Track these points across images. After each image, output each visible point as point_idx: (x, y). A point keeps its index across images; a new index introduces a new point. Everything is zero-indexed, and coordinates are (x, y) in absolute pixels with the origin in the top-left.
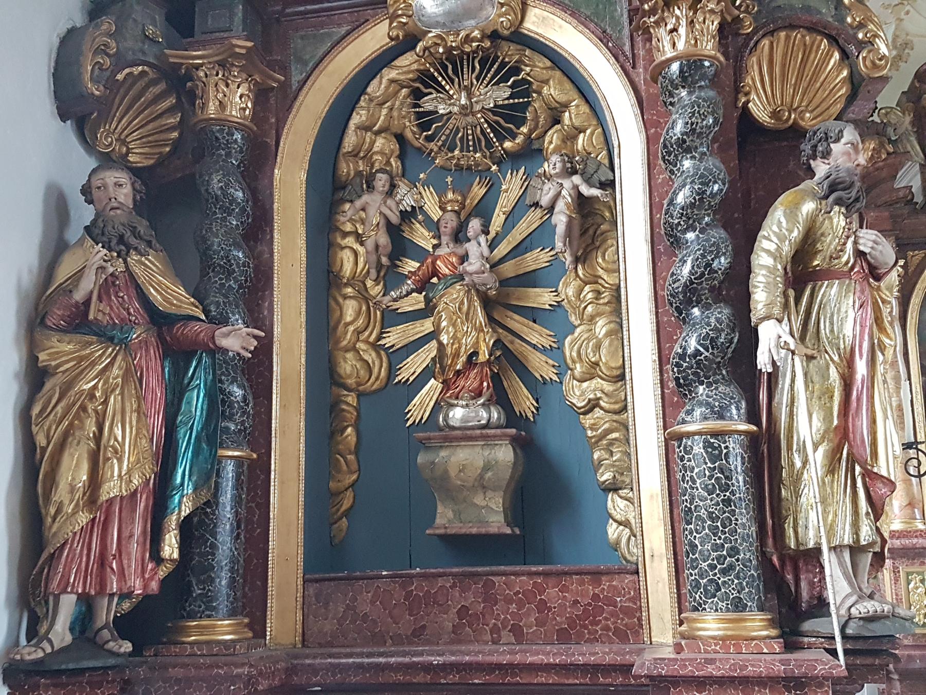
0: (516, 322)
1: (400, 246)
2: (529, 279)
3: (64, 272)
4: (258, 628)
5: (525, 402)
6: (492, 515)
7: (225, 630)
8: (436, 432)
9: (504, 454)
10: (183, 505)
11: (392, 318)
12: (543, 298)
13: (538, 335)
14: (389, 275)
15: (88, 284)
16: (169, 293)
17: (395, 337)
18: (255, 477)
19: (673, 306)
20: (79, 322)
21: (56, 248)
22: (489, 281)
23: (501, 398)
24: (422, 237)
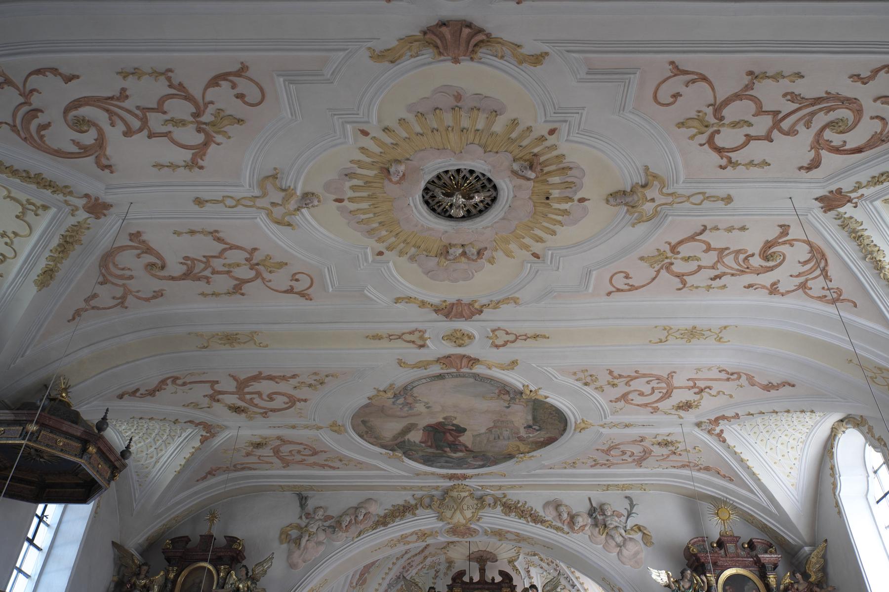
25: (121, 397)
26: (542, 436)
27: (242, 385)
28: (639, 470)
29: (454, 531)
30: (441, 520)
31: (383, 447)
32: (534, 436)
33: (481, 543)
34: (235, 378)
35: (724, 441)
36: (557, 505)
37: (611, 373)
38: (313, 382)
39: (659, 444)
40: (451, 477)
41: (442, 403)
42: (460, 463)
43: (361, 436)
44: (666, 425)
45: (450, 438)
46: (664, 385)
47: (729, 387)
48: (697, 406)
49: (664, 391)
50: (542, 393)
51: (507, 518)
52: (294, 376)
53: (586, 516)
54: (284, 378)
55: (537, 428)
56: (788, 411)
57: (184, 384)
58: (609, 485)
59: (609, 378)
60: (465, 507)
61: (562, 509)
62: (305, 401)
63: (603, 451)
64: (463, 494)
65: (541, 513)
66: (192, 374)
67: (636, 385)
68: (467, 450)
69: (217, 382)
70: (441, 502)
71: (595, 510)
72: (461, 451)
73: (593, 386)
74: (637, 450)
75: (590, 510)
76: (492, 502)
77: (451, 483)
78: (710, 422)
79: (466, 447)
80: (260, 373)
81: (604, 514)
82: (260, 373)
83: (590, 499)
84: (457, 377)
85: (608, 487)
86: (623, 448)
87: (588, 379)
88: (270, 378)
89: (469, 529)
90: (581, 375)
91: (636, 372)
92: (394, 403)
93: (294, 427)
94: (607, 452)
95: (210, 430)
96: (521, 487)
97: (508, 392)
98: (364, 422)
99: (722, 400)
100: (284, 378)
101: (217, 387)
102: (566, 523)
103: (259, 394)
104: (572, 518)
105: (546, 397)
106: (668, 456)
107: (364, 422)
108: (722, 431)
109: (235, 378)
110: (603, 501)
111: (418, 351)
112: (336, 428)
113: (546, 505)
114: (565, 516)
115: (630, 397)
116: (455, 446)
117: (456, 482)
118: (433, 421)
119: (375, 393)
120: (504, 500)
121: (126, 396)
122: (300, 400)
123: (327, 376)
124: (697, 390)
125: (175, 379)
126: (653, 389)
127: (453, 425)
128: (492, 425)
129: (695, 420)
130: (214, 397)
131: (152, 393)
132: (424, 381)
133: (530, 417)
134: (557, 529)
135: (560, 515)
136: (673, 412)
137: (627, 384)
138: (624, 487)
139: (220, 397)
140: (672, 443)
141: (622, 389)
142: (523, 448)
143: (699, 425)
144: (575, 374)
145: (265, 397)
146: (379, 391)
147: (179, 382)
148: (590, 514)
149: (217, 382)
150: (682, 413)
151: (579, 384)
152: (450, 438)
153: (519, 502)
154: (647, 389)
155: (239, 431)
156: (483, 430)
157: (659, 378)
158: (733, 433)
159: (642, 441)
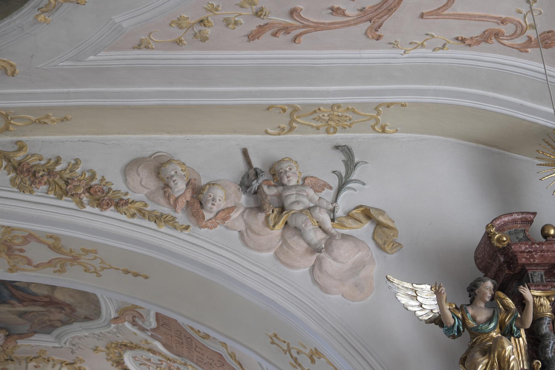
28: (376, 55)
36: (159, 167)
51: (26, 197)
53: (234, 188)
58: (295, 109)
61: (170, 170)
65: (118, 184)
71: (257, 174)
75: (247, 175)
83: (245, 152)
102: (182, 203)
104: (198, 196)
110: (279, 155)
113: (135, 164)
114: (180, 187)
120: (19, 157)
134: (158, 218)
135: (167, 186)
138: (332, 118)
148: (245, 185)
153: (58, 161)
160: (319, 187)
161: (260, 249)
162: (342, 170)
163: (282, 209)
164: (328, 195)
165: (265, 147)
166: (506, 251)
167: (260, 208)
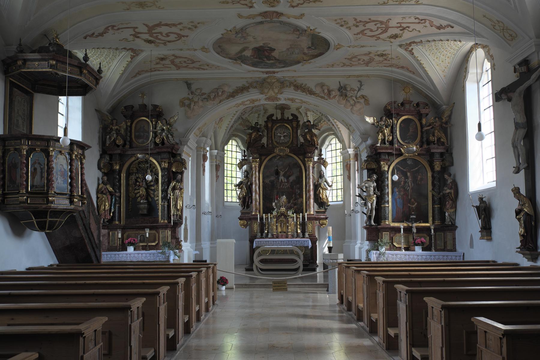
0: (150, 191)
1: (136, 181)
2: (152, 186)
3: (100, 187)
4: (120, 223)
5: (150, 200)
6: (145, 212)
7: (117, 223)
8: (140, 203)
9: (146, 206)
10: (113, 210)
11: (136, 189)
12: (153, 188)
13: (152, 192)
14: (136, 185)
15: (103, 189)
16: (111, 189)
17: (136, 191)
18: (120, 208)
19: (162, 191)
20: (102, 193)
21: (99, 185)
22: (146, 187)
23: (147, 199)
24: (139, 180)
25: (85, 38)
26: (315, 52)
27: (151, 29)
29: (268, 99)
30: (262, 94)
31: (230, 58)
32: (312, 52)
33: (282, 102)
34: (147, 25)
35: (413, 54)
36: (322, 85)
37: (355, 19)
38: (190, 27)
39: (378, 55)
40: (267, 73)
41: (261, 36)
42: (272, 66)
43: (218, 54)
44: (383, 47)
45: (267, 54)
46: (384, 26)
47: (418, 27)
48: (401, 37)
49: (384, 29)
50: (317, 30)
52: (180, 24)
54: (174, 25)
55: (313, 48)
56: (448, 40)
57: (119, 29)
58: (350, 75)
59: (355, 22)
60: (274, 87)
61: (324, 87)
62: (187, 36)
63: (348, 59)
64: (273, 81)
65: (314, 90)
66: (122, 24)
67: (368, 26)
68: (276, 59)
69: (137, 28)
70: (261, 85)
72: (272, 60)
73: (345, 27)
74: (366, 58)
76: (288, 84)
77: (267, 75)
78: (407, 44)
79: (275, 58)
80: (161, 22)
81: (346, 90)
82: (161, 22)
83: (340, 82)
84: (270, 22)
85: (350, 76)
86: (359, 57)
87: (343, 24)
88: (166, 25)
89: (277, 98)
90: (339, 21)
91: (370, 19)
92: (236, 37)
93: (181, 50)
94: (350, 59)
95: (135, 52)
96: (304, 77)
97: (299, 30)
98: (219, 46)
99: (415, 33)
100: (174, 25)
101: (136, 30)
103: (161, 33)
104: (329, 92)
105: (319, 33)
106: (383, 61)
107: (219, 46)
108: (412, 49)
109: (147, 25)
111: (248, 9)
112: (204, 49)
115: (365, 32)
116: (269, 58)
117: (270, 75)
118: (257, 45)
119: (225, 31)
120: (295, 83)
121: (88, 37)
122: (184, 36)
123: (199, 23)
124: (401, 28)
125: (113, 27)
126: (378, 28)
127: (268, 47)
128: (289, 47)
129: (399, 44)
130: (136, 35)
131: (101, 35)
132: (252, 25)
133: (310, 43)
134: (322, 97)
136: (388, 39)
137: (364, 26)
138: (358, 76)
139: (139, 35)
140: (385, 55)
141: (361, 28)
142: (305, 58)
143: (400, 46)
144: (336, 20)
145: (164, 35)
146: (228, 31)
147: (115, 28)
148: (339, 90)
149: (137, 28)
150: (392, 40)
151: (338, 26)
152: (267, 54)
154: (374, 28)
155: (150, 52)
156: (284, 49)
157: (382, 23)
158: (418, 50)
159: (369, 54)
160: (354, 90)
161: (341, 104)
162: (359, 86)
163: (346, 96)
164: (356, 92)
165: (344, 82)
166: (389, 110)
167: (342, 95)
